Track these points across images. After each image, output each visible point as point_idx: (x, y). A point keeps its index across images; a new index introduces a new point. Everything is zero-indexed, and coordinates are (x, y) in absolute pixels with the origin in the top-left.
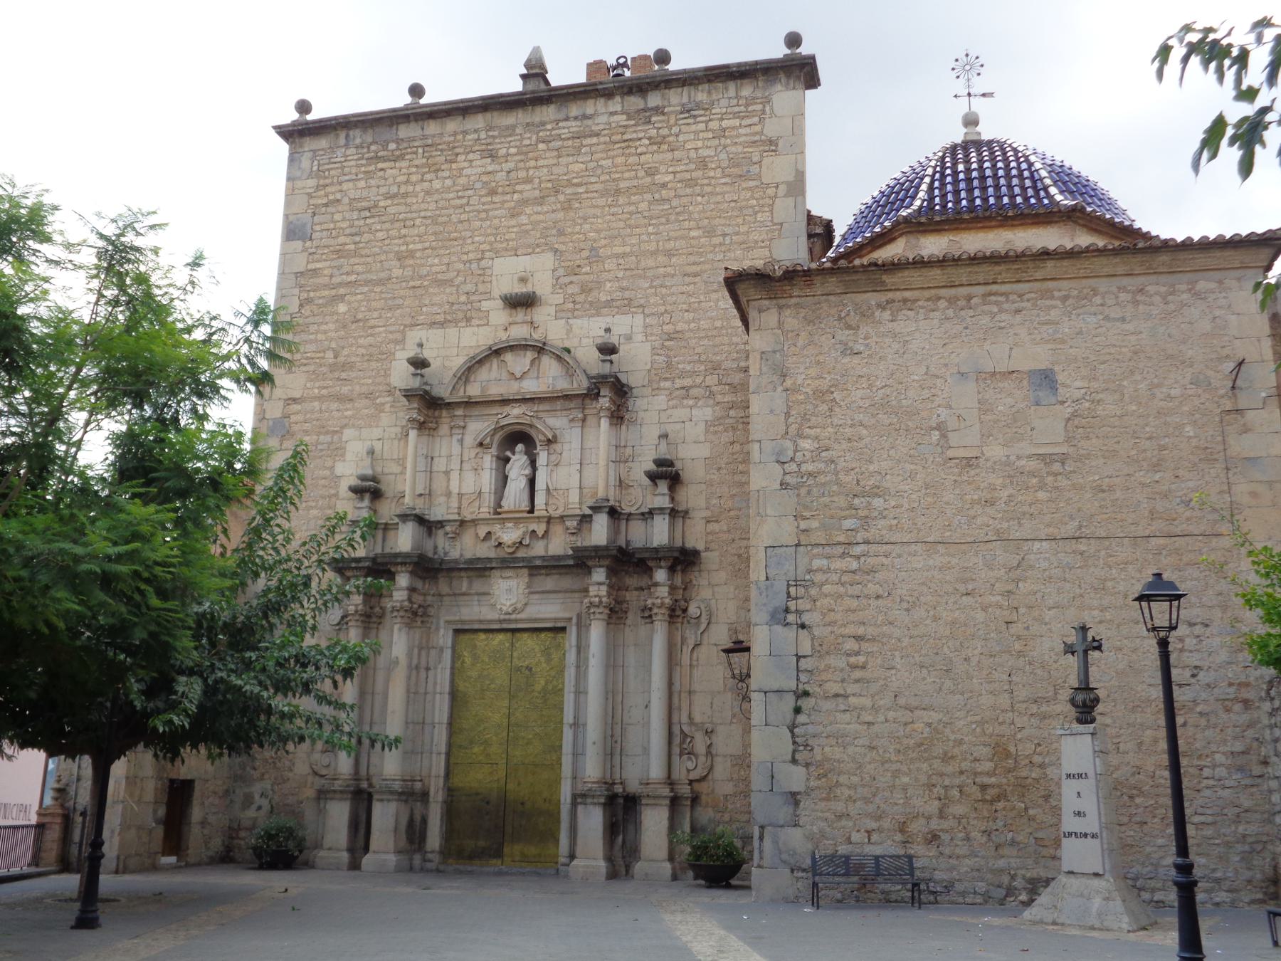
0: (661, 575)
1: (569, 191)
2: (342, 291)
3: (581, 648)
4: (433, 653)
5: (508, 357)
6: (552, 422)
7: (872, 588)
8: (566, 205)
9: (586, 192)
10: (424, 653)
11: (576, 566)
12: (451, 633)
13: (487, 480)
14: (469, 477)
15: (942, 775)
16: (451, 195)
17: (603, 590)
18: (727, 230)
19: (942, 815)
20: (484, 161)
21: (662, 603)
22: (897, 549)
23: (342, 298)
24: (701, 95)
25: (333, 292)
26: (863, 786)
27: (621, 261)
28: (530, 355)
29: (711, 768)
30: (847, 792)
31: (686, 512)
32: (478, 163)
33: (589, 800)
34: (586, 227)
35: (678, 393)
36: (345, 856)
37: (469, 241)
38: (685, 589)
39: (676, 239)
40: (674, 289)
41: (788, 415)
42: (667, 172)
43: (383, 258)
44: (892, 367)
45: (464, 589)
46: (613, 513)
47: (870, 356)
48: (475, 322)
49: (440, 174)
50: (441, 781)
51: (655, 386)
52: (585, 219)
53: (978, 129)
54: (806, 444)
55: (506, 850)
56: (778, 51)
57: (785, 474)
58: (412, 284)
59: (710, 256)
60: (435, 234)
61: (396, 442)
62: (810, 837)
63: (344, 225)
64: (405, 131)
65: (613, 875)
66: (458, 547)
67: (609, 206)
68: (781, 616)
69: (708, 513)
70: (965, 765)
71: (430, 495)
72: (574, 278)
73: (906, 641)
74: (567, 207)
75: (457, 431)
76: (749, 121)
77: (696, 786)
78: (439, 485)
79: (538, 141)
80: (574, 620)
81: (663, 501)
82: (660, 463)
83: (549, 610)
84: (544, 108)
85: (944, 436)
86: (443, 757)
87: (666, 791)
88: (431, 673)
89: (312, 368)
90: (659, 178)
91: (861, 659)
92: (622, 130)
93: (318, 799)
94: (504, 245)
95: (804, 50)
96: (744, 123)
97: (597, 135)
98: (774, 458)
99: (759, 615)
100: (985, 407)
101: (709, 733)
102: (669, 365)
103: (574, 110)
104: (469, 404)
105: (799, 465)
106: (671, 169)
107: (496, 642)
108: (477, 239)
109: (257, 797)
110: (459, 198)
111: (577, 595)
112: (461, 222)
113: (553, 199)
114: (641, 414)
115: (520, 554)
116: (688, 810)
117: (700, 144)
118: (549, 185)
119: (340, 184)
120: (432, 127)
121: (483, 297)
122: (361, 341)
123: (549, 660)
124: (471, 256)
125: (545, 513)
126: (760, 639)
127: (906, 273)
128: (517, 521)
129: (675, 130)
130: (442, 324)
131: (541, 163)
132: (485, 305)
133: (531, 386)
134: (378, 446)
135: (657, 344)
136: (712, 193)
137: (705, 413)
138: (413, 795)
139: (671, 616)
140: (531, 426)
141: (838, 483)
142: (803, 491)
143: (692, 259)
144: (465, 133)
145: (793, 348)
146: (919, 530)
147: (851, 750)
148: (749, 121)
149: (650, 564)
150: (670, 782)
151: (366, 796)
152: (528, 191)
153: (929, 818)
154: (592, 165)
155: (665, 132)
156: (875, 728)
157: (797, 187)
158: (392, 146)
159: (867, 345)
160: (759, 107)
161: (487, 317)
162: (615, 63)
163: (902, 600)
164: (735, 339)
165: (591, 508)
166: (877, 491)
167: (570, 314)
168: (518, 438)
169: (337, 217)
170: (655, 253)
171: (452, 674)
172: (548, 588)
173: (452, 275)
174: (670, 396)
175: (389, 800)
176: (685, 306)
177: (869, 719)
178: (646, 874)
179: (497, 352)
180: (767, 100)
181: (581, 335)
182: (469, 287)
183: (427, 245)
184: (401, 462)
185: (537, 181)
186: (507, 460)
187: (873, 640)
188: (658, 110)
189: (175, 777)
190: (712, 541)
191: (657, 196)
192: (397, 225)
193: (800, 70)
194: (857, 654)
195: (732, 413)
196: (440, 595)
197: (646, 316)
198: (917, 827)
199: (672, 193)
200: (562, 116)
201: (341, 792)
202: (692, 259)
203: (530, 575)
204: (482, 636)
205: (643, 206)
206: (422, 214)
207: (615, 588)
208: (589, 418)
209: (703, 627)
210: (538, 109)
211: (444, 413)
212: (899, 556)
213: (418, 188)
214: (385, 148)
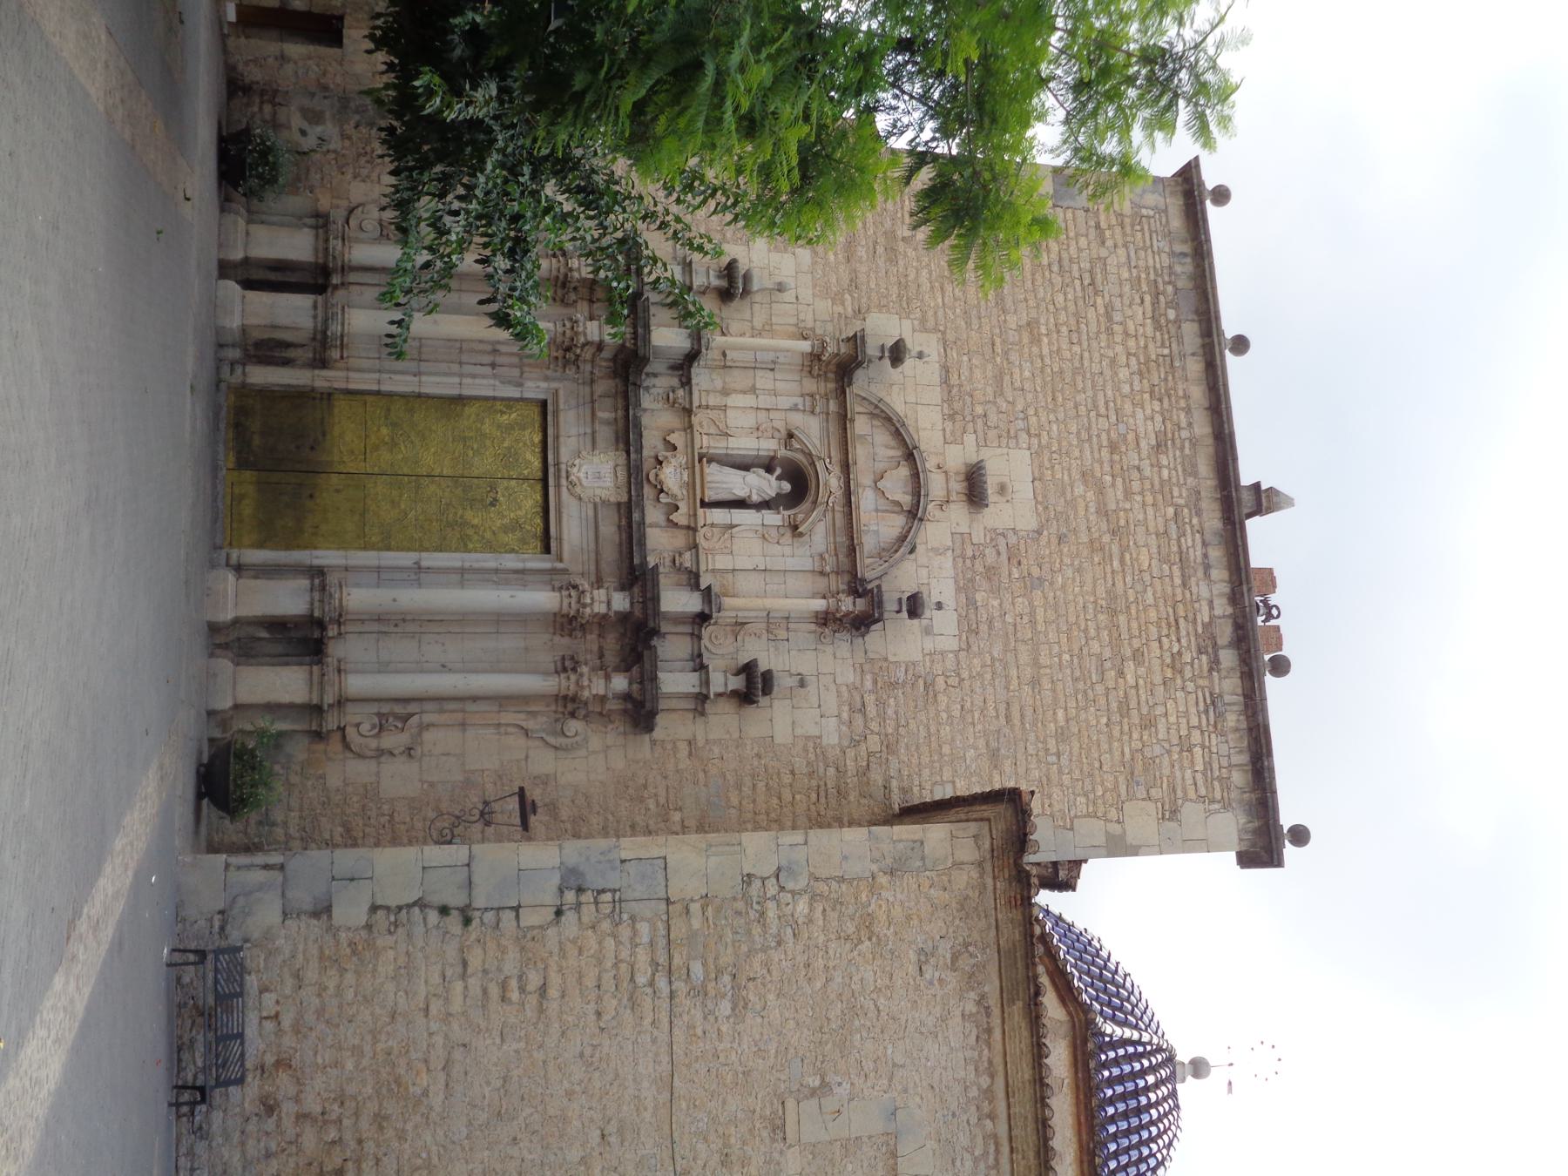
0: (620, 683)
1: (1115, 549)
3: (521, 576)
4: (516, 372)
5: (904, 471)
6: (820, 529)
7: (610, 1004)
8: (1097, 545)
9: (1113, 572)
11: (632, 568)
12: (542, 397)
13: (744, 445)
14: (749, 420)
15: (357, 1114)
16: (1109, 393)
17: (601, 608)
18: (1064, 760)
19: (302, 1117)
20: (1153, 436)
21: (582, 688)
22: (663, 1037)
24: (1233, 719)
26: (340, 1007)
27: (1026, 619)
28: (906, 500)
29: (360, 756)
30: (331, 984)
31: (703, 714)
32: (1150, 428)
33: (317, 595)
34: (1069, 573)
35: (858, 698)
36: (238, 255)
37: (1052, 417)
38: (601, 714)
39: (1054, 691)
40: (990, 690)
41: (841, 880)
42: (1137, 677)
43: (1032, 303)
44: (903, 1018)
45: (600, 414)
46: (703, 618)
47: (917, 988)
49: (1136, 378)
50: (343, 385)
51: (866, 667)
52: (1079, 570)
53: (1189, 1079)
54: (802, 906)
55: (248, 475)
56: (1287, 820)
57: (763, 880)
58: (998, 341)
59: (1032, 737)
60: (1061, 372)
61: (793, 320)
62: (268, 935)
63: (1073, 250)
64: (1190, 330)
65: (214, 628)
66: (654, 406)
67: (1095, 602)
68: (573, 881)
69: (700, 744)
70: (370, 1147)
71: (725, 367)
72: (1004, 557)
73: (539, 1056)
74: (1095, 546)
75: (808, 404)
76: (1200, 782)
77: (338, 735)
78: (738, 379)
79: (1177, 506)
80: (559, 565)
81: (718, 682)
82: (768, 677)
83: (573, 529)
84: (1218, 514)
85: (813, 1092)
86: (375, 388)
87: (329, 699)
88: (488, 370)
90: (1130, 667)
91: (515, 995)
92: (1191, 616)
93: (317, 215)
94: (1047, 464)
95: (1289, 851)
96: (1199, 776)
97: (1184, 585)
98: (784, 863)
99: (573, 851)
100: (850, 1145)
101: (409, 751)
102: (893, 685)
103: (1216, 554)
104: (844, 419)
105: (774, 898)
106: (1141, 682)
107: (529, 456)
108: (1055, 427)
109: (319, 129)
110: (1106, 403)
111: (593, 568)
112: (1076, 407)
113: (1104, 526)
114: (829, 649)
116: (305, 727)
117: (1172, 719)
118: (1122, 522)
119: (1125, 245)
120: (1195, 367)
121: (981, 434)
122: (924, 273)
123: (506, 529)
124: (1033, 420)
125: (701, 523)
126: (542, 857)
127: (1026, 1033)
128: (691, 486)
129: (1190, 686)
130: (945, 381)
131: (1150, 511)
132: (970, 439)
133: (866, 501)
134: (789, 296)
135: (921, 670)
136: (1111, 736)
137: (832, 735)
138: (323, 348)
139: (565, 697)
140: (815, 502)
141: (750, 953)
142: (740, 905)
143: (1029, 712)
144: (1188, 410)
145: (927, 884)
146: (688, 1066)
147: (390, 987)
148: (1200, 782)
149: (635, 669)
150: (341, 702)
151: (320, 281)
152: (1114, 496)
153: (297, 1100)
154: (1147, 578)
155: (1188, 674)
156: (420, 1020)
157: (1119, 847)
158: (1172, 314)
159: (931, 983)
160: (1218, 795)
161: (954, 442)
162: (1271, 603)
163: (594, 1047)
164: (926, 772)
165: (709, 588)
166: (740, 1006)
167: (958, 552)
169: (1083, 242)
170: (1036, 663)
171: (487, 399)
172: (602, 528)
173: (1009, 395)
174: (852, 688)
175: (315, 317)
176: (968, 705)
177: (433, 1010)
178: (215, 675)
179: (910, 455)
180: (1226, 806)
181: (931, 569)
182: (993, 418)
183: (1047, 361)
184: (768, 329)
185: (1128, 506)
186: (769, 469)
187: (541, 1010)
188: (1215, 663)
189: (346, 23)
190: (664, 749)
191: (1108, 665)
192: (1072, 321)
193: (1264, 845)
194: (522, 989)
195: (831, 771)
196: (592, 381)
197: (956, 653)
198: (284, 1083)
199: (1111, 684)
200: (1208, 537)
201: (326, 249)
202: (1029, 712)
203: (619, 504)
204: (537, 438)
205: (1095, 647)
206: (1086, 355)
207: (602, 621)
209: (551, 740)
210: (1216, 506)
211: (831, 386)
212: (654, 1041)
213: (1119, 349)
214: (1169, 305)
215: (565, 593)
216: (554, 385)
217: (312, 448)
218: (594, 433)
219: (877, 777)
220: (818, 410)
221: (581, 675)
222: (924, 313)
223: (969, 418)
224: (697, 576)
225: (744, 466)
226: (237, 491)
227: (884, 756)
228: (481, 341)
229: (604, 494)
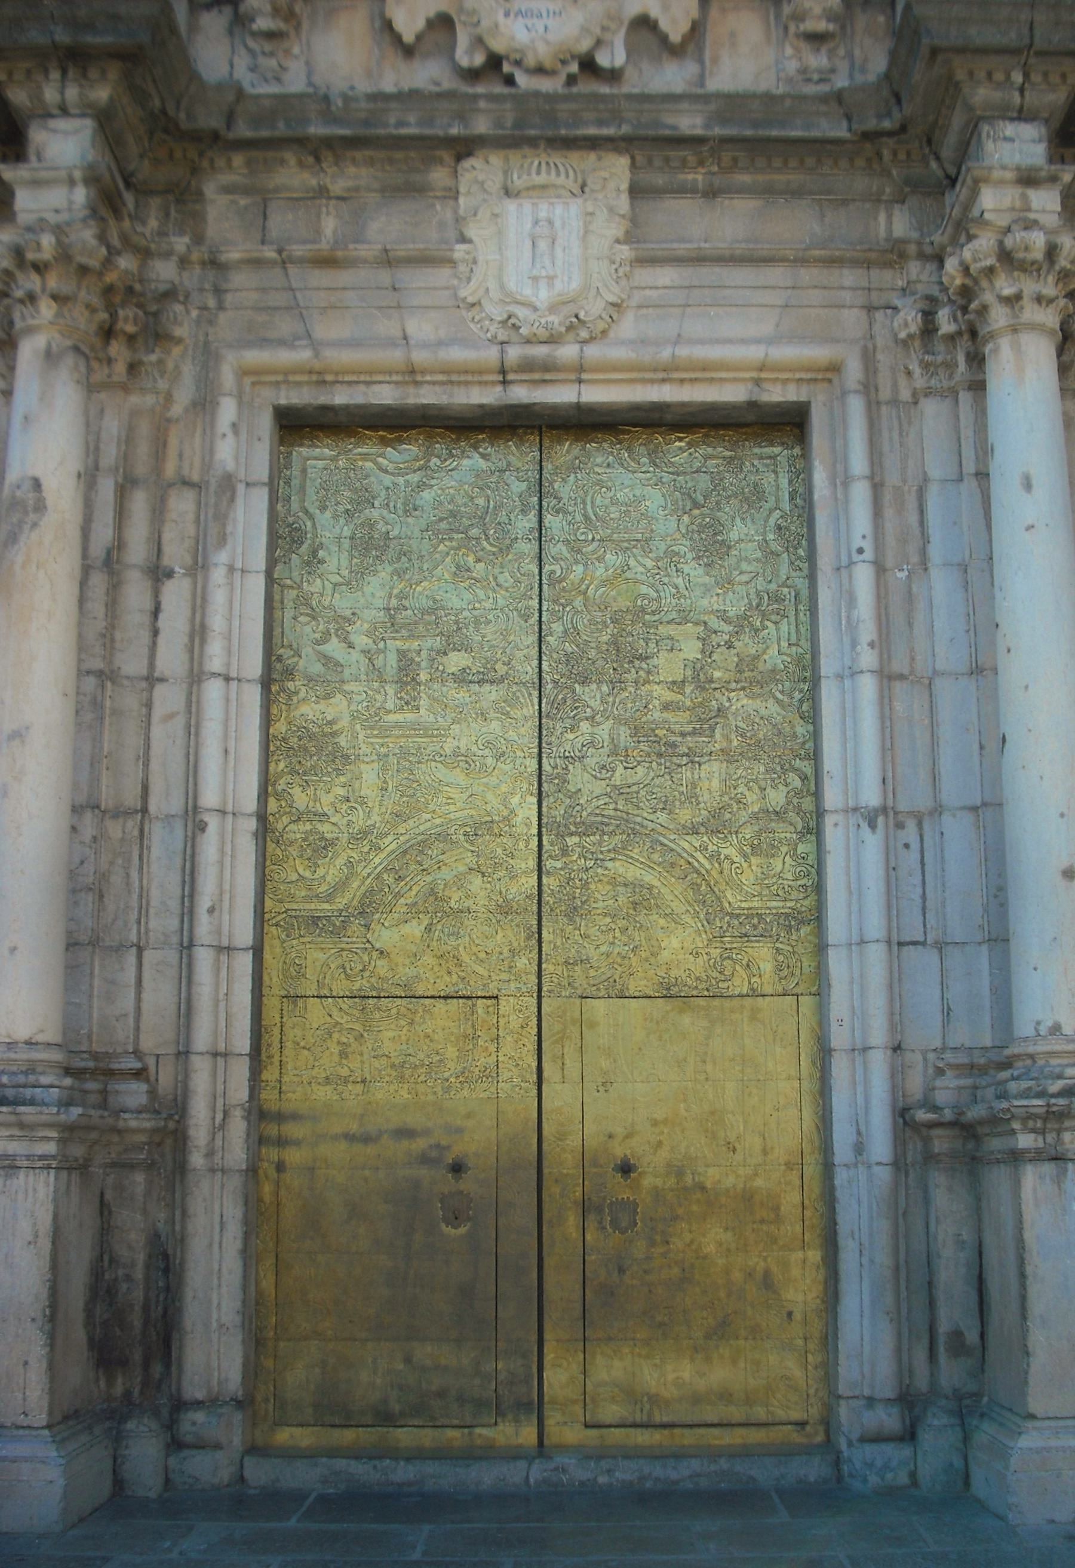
4: (182, 505)
10: (139, 503)
12: (265, 423)
50: (241, 1071)
80: (854, 371)
86: (244, 962)
88: (176, 594)
123: (713, 547)
203: (636, 191)
215: (999, 317)
216: (227, 377)
217: (457, 1168)
226: (611, 1412)
228: (82, 601)
229: (608, 229)
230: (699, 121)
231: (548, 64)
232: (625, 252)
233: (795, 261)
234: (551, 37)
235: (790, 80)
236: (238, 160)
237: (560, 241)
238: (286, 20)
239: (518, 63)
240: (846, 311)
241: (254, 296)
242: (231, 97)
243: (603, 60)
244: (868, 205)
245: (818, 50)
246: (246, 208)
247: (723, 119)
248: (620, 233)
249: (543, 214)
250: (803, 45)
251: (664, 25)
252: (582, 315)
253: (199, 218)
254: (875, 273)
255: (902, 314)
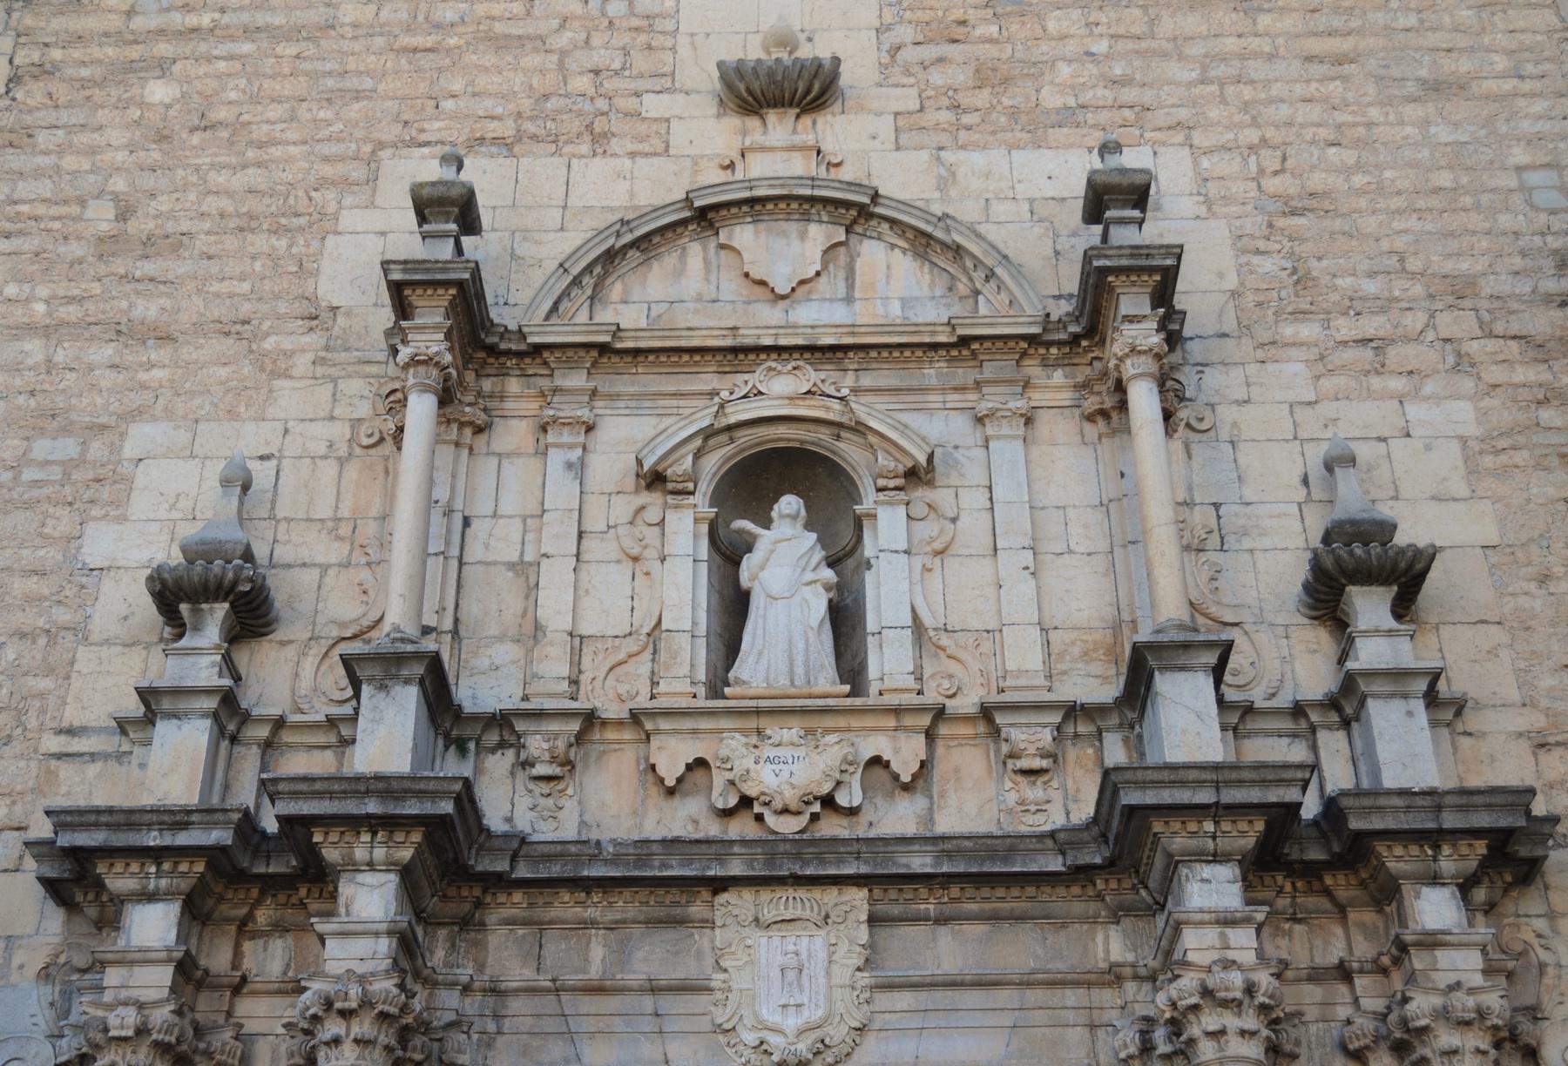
2: (164, 49)
5: (743, 235)
13: (683, 592)
23: (162, 68)
25: (134, 52)
28: (819, 234)
35: (1349, 354)
45: (594, 972)
48: (615, 145)
51: (1264, 335)
61: (329, 469)
69: (1540, 721)
71: (455, 632)
75: (566, 437)
78: (490, 604)
89: (29, 244)
104: (604, 352)
111: (1072, 997)
114: (1227, 414)
115: (832, 827)
122: (221, 179)
125: (911, 699)
132: (653, 106)
133: (821, 317)
135: (1253, 224)
137: (1450, 414)
149: (1397, 859)
164: (1505, 221)
167: (944, 138)
168: (776, 471)
174: (1322, 365)
176: (1323, 133)
179: (705, 217)
182: (599, 57)
186: (746, 545)
197: (1197, 153)
202: (1321, 21)
203: (873, 920)
208: (1043, 417)
211: (513, 385)
218: (654, 989)
219: (1542, 323)
220: (584, 414)
221: (1443, 1014)
222: (323, 183)
223: (602, 104)
224: (1073, 711)
225: (733, 607)
227: (1486, 304)
230: (928, 860)
231: (793, 806)
232: (865, 978)
233: (1020, 984)
234: (793, 781)
235: (1010, 812)
236: (518, 896)
237: (805, 972)
238: (562, 765)
239: (766, 804)
240: (1070, 1030)
241: (529, 1021)
242: (515, 845)
243: (842, 800)
244: (1085, 927)
245: (1034, 783)
246: (524, 936)
247: (949, 855)
248: (860, 962)
249: (791, 948)
250: (1019, 778)
251: (894, 766)
252: (827, 1041)
253: (480, 945)
254: (1095, 992)
255: (1121, 1035)
